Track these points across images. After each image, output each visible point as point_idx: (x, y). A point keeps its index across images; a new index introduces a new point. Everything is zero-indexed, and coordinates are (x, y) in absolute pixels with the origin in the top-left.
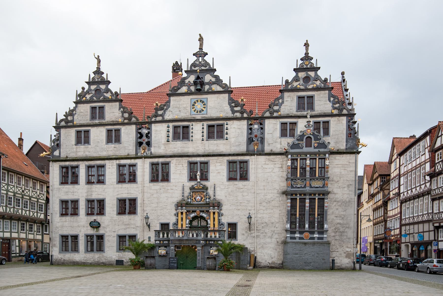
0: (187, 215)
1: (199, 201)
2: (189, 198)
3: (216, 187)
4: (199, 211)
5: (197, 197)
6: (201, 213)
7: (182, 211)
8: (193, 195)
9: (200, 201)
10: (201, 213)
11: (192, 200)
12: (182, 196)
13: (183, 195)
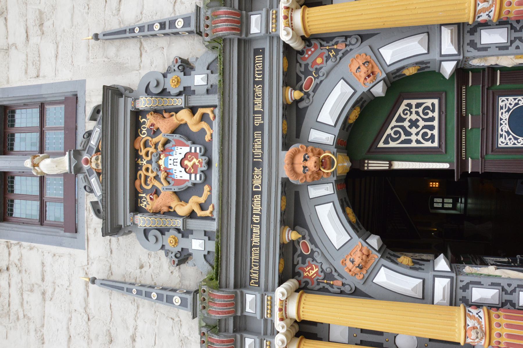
0: (329, 276)
1: (199, 162)
2: (183, 243)
3: (116, 27)
4: (285, 155)
5: (168, 174)
6: (315, 135)
7: (279, 326)
8: (156, 213)
9: (207, 152)
10: (315, 135)
11: (192, 224)
12: (163, 307)
13: (160, 298)
